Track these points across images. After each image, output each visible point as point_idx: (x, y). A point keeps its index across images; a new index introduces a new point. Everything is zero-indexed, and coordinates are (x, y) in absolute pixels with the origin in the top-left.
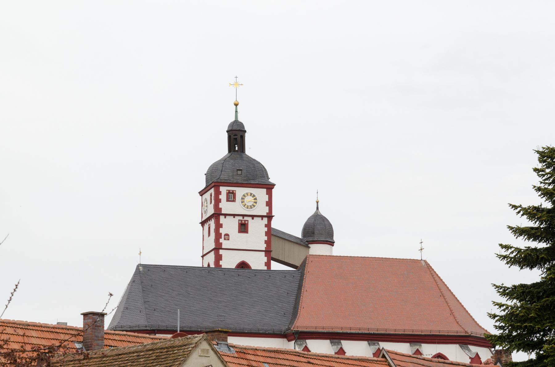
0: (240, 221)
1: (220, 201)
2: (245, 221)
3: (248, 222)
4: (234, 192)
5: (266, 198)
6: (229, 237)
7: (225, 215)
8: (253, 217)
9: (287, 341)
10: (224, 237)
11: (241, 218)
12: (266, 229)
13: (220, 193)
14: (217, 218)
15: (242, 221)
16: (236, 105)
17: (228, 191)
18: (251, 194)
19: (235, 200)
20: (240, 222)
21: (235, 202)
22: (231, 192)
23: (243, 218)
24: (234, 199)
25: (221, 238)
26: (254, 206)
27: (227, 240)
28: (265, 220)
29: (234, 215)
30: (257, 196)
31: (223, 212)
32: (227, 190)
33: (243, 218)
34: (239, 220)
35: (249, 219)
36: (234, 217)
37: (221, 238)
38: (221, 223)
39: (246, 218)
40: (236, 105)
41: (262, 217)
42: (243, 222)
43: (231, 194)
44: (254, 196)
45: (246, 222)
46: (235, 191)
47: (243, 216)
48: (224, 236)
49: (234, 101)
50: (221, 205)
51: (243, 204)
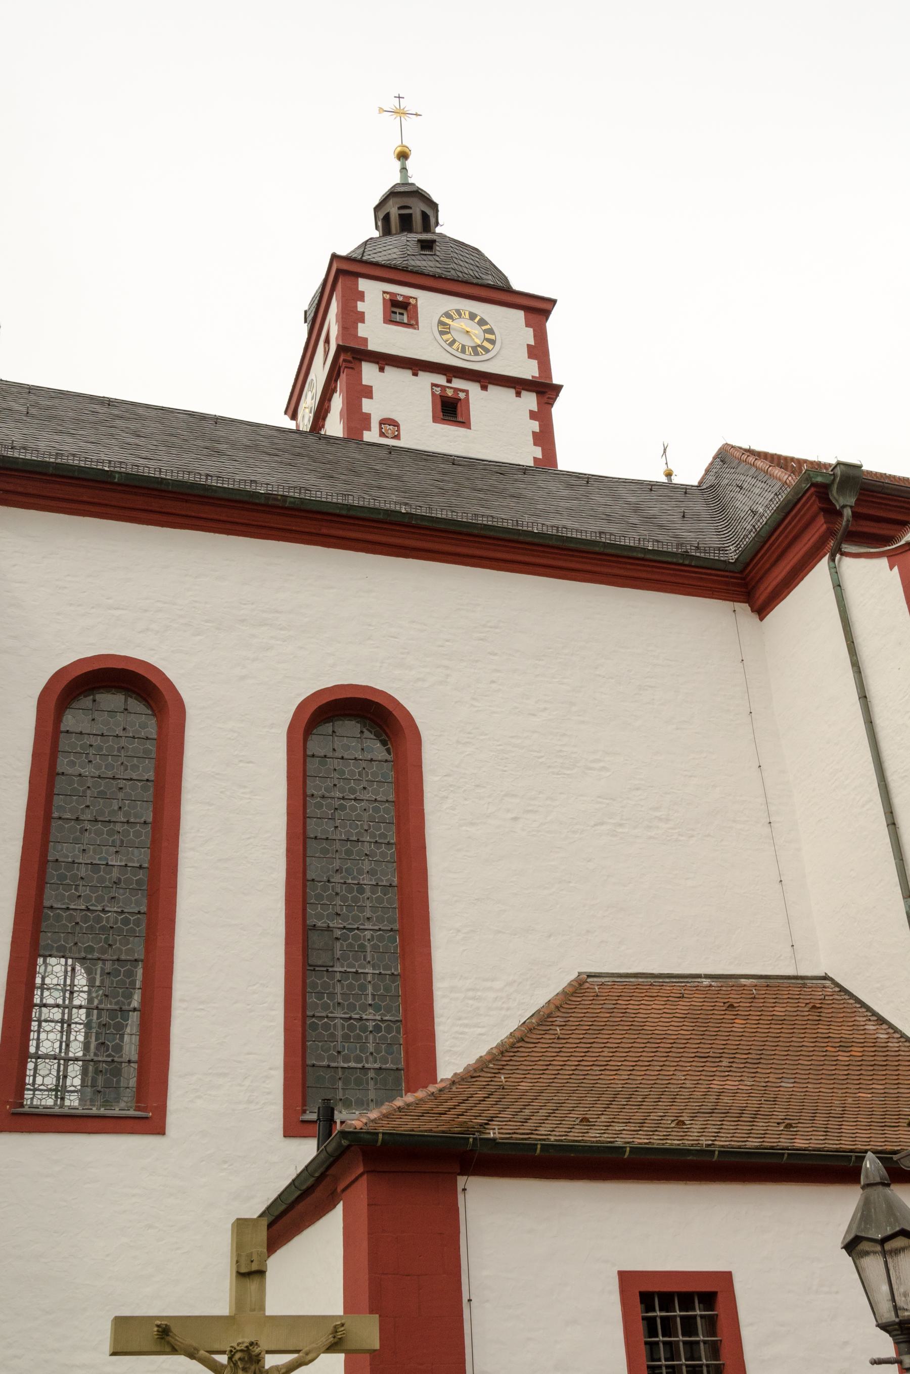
0: (439, 389)
1: (361, 317)
2: (456, 390)
3: (467, 395)
4: (412, 301)
5: (528, 336)
6: (398, 430)
7: (384, 360)
8: (486, 379)
9: (755, 617)
10: (381, 428)
11: (441, 380)
12: (535, 426)
13: (361, 296)
14: (352, 368)
15: (443, 388)
16: (403, 156)
17: (387, 297)
18: (472, 316)
19: (417, 323)
20: (438, 393)
21: (415, 329)
22: (400, 299)
23: (449, 381)
24: (413, 322)
25: (369, 429)
26: (487, 351)
27: (392, 438)
28: (530, 401)
29: (416, 366)
30: (492, 324)
31: (371, 347)
32: (384, 292)
33: (449, 381)
34: (433, 385)
35: (473, 389)
36: (415, 374)
37: (369, 429)
38: (364, 382)
39: (458, 383)
40: (403, 156)
41: (517, 385)
42: (450, 393)
43: (398, 310)
44: (482, 322)
45: (462, 395)
46: (416, 299)
47: (451, 372)
48: (381, 424)
49: (394, 146)
50: (362, 330)
51: (445, 337)
